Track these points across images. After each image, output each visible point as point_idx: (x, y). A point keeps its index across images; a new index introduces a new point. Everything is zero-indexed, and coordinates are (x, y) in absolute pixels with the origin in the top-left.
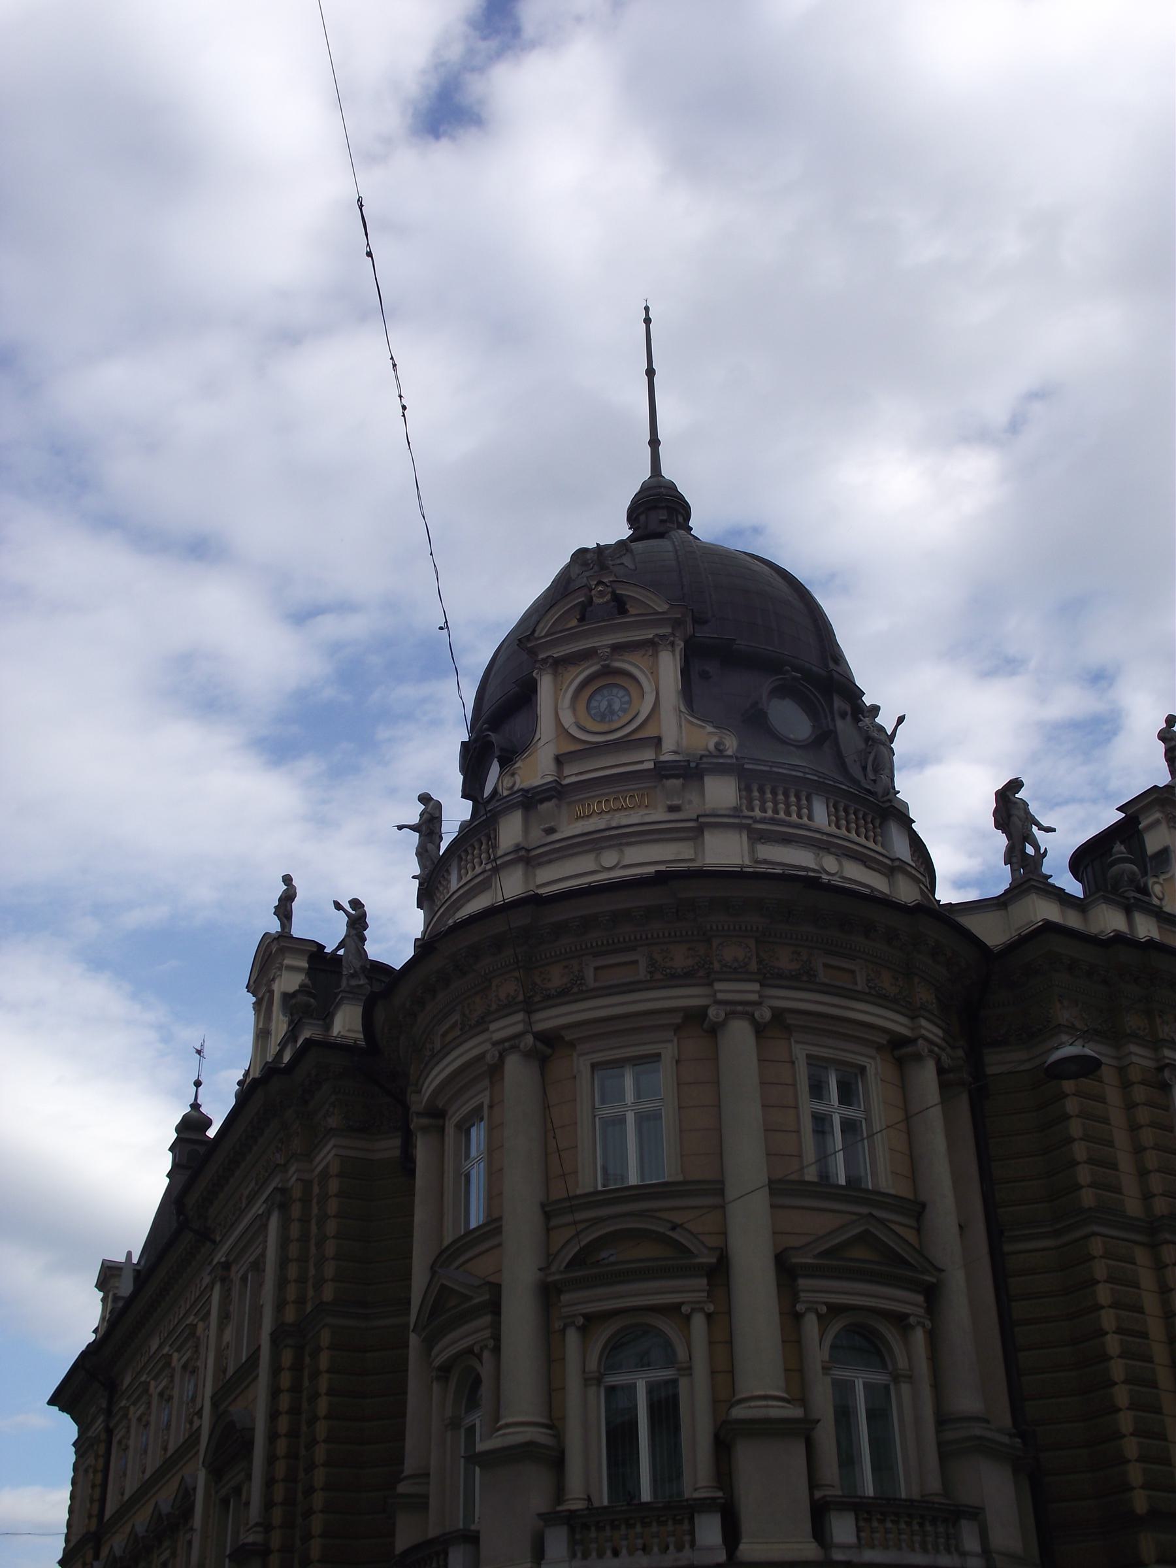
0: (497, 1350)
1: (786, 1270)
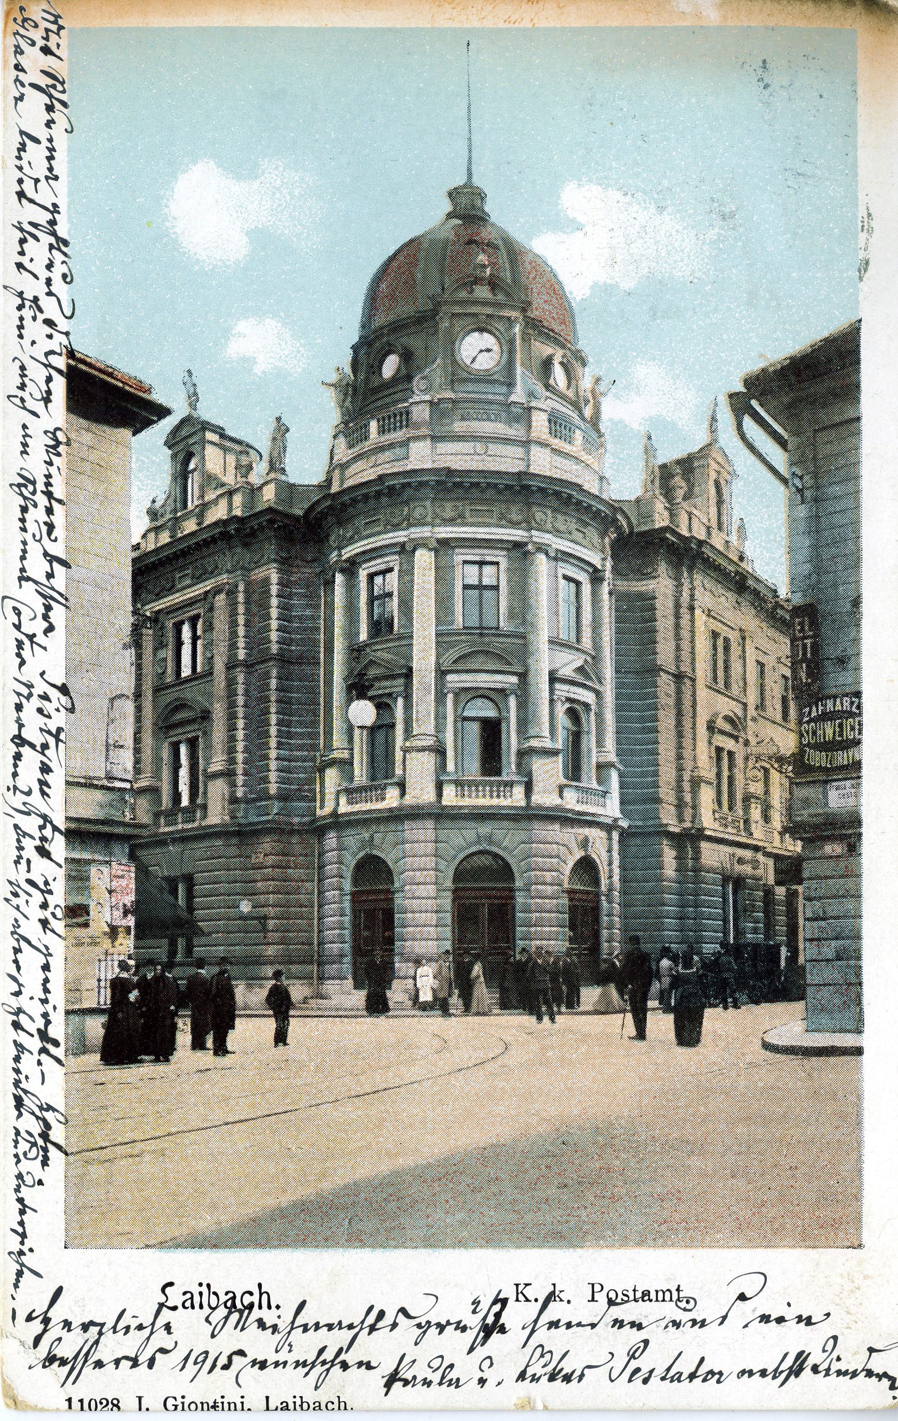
0: (408, 697)
1: (553, 678)
